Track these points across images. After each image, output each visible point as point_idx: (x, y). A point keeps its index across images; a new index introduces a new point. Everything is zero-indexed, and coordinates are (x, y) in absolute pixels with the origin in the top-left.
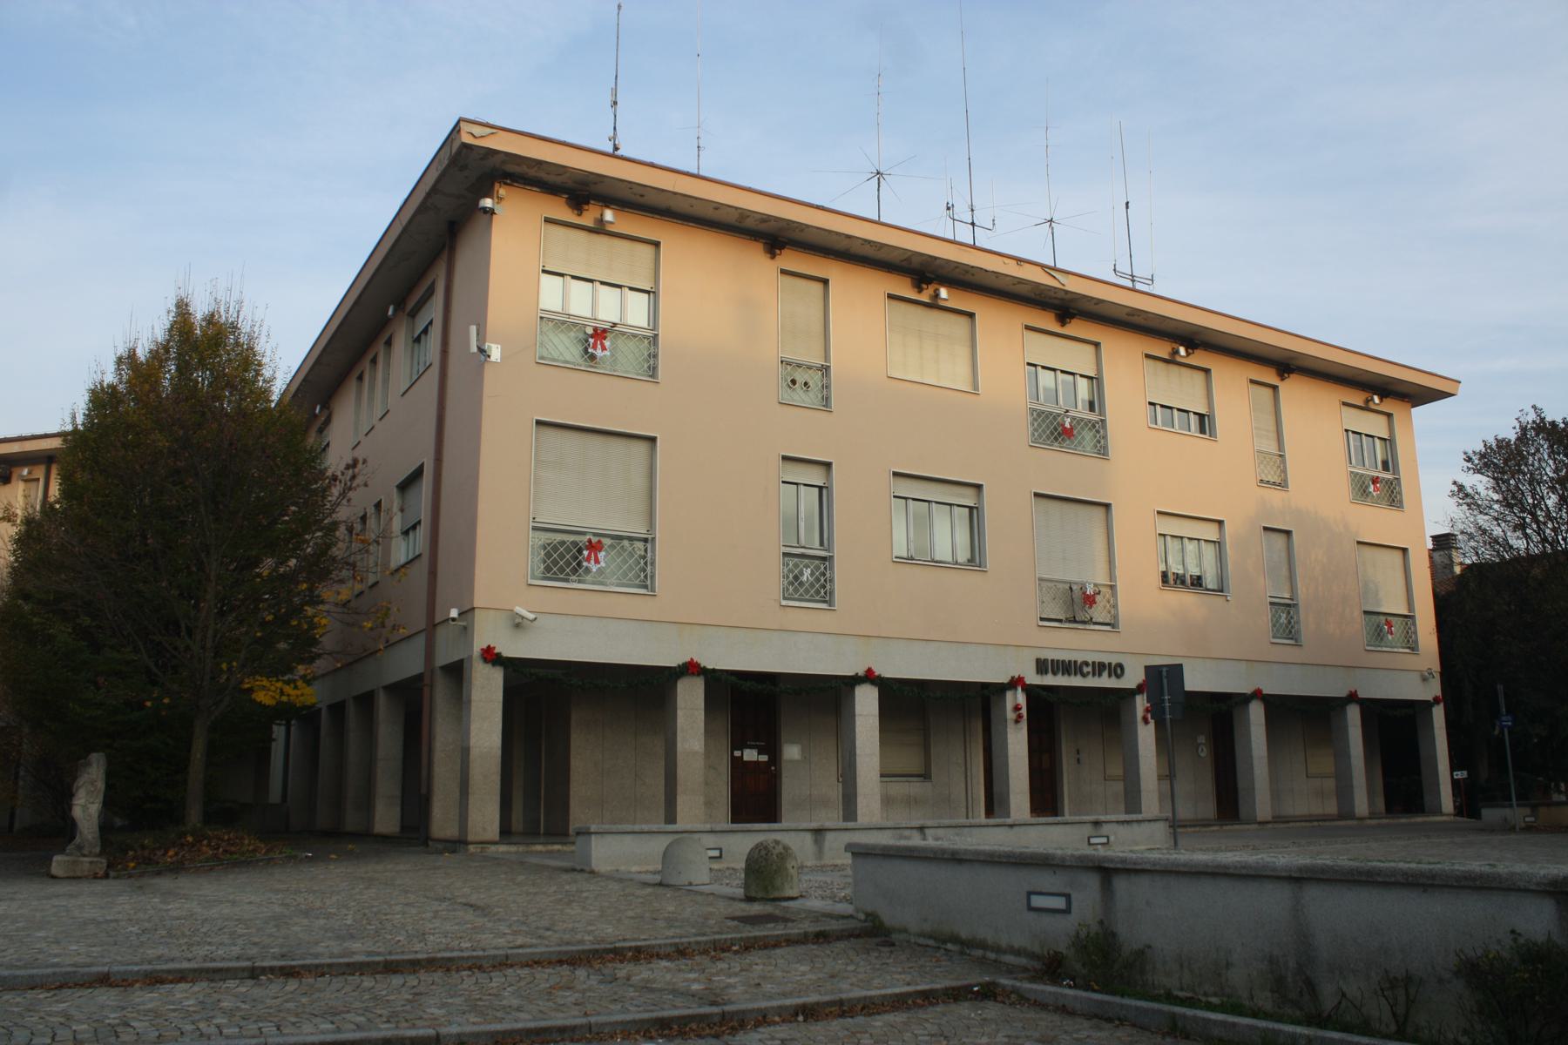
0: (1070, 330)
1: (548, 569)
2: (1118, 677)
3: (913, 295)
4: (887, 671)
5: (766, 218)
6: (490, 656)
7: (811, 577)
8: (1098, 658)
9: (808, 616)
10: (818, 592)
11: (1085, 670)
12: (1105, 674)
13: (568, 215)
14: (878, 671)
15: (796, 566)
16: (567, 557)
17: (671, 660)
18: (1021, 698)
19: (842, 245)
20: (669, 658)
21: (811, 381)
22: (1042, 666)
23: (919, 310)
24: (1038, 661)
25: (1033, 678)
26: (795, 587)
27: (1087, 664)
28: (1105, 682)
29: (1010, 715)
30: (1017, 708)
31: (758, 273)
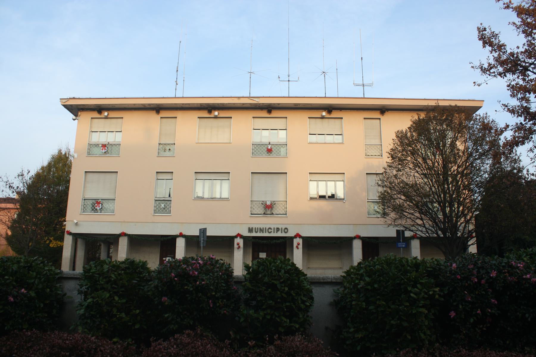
0: (332, 116)
1: (93, 210)
2: (286, 233)
3: (208, 116)
4: (304, 235)
5: (149, 105)
6: (69, 233)
7: (163, 205)
8: (276, 227)
9: (162, 218)
10: (166, 211)
11: (270, 230)
12: (280, 231)
13: (97, 115)
14: (184, 233)
15: (159, 203)
16: (96, 205)
17: (118, 232)
18: (300, 241)
19: (175, 106)
20: (116, 231)
21: (165, 148)
22: (250, 230)
23: (212, 119)
24: (249, 228)
25: (246, 234)
26: (157, 210)
27: (270, 228)
28: (279, 234)
29: (236, 246)
30: (299, 244)
31: (153, 119)
